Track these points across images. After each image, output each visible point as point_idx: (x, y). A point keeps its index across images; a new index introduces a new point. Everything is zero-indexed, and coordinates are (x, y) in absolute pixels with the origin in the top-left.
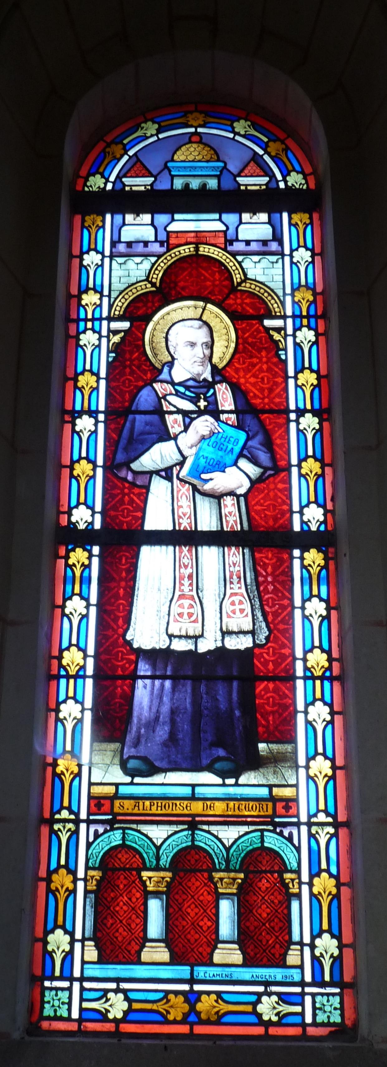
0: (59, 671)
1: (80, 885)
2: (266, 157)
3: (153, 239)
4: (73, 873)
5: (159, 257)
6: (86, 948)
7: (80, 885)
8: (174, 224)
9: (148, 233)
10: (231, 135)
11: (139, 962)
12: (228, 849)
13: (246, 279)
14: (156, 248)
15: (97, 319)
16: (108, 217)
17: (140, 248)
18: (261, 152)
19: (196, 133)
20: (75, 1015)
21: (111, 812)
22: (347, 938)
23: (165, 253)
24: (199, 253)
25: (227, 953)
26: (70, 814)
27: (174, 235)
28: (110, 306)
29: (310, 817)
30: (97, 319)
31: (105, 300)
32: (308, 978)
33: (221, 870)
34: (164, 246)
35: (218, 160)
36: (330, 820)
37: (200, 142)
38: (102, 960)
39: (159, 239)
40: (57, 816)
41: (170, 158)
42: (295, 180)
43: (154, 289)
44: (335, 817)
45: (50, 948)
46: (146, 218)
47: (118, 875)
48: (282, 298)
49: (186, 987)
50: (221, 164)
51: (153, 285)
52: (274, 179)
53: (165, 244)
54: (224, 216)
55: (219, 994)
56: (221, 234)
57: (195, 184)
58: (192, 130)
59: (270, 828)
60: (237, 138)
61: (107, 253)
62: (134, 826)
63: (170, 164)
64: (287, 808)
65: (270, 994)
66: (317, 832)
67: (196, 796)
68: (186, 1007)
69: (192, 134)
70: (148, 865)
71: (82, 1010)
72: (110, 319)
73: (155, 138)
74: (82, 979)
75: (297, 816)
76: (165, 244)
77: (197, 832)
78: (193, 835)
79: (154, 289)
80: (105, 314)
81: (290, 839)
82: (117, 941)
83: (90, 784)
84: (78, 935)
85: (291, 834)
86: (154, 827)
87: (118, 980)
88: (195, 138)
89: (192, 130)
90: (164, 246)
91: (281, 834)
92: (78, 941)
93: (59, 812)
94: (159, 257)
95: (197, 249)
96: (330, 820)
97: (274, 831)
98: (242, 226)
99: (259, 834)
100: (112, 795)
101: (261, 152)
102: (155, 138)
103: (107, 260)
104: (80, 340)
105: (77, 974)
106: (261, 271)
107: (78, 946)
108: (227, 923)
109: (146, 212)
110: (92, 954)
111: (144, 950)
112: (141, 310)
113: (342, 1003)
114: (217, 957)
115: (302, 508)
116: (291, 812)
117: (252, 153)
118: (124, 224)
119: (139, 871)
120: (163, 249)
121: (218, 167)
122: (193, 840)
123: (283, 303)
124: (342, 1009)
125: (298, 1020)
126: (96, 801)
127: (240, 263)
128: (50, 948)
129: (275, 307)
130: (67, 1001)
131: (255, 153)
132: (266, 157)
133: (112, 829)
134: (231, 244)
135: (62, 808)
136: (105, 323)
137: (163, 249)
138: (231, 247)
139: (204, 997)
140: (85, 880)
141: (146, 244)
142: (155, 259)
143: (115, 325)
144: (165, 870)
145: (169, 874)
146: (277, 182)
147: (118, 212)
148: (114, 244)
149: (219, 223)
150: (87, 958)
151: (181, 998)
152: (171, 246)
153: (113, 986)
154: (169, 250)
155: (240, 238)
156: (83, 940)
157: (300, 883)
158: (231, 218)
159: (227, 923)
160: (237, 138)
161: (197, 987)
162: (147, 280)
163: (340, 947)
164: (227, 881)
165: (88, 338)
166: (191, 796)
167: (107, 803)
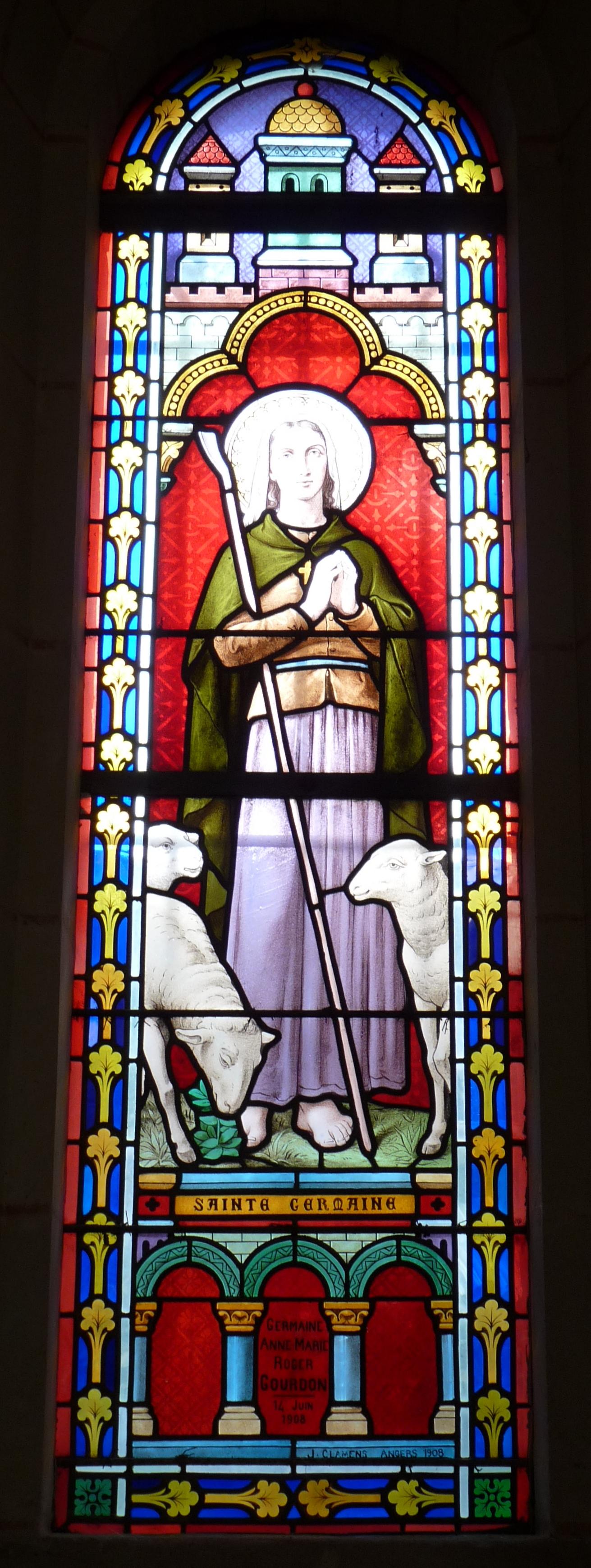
0: (87, 1003)
1: (125, 1323)
2: (423, 129)
3: (232, 280)
4: (116, 1306)
5: (242, 310)
6: (134, 1416)
7: (125, 1323)
8: (269, 252)
9: (223, 270)
10: (365, 84)
11: (214, 1435)
12: (347, 1266)
13: (386, 351)
14: (236, 295)
15: (141, 418)
16: (158, 237)
17: (208, 295)
18: (415, 118)
19: (305, 79)
20: (121, 1512)
21: (171, 1215)
22: (522, 1398)
23: (251, 305)
24: (309, 304)
25: (347, 1422)
26: (108, 1220)
27: (267, 272)
28: (163, 394)
29: (471, 1217)
30: (141, 418)
31: (154, 389)
32: (465, 1453)
33: (336, 1299)
34: (250, 293)
35: (343, 134)
36: (500, 1224)
37: (313, 96)
38: (158, 1435)
39: (241, 281)
40: (89, 1223)
41: (262, 129)
42: (470, 176)
43: (234, 367)
44: (508, 1218)
45: (81, 1417)
46: (220, 241)
47: (182, 1301)
48: (443, 387)
49: (286, 1470)
50: (347, 142)
51: (232, 359)
52: (434, 172)
53: (253, 289)
54: (350, 237)
55: (333, 1479)
56: (345, 273)
57: (304, 182)
58: (300, 72)
59: (413, 1235)
60: (377, 90)
61: (156, 305)
62: (208, 1236)
63: (262, 141)
64: (438, 1204)
65: (408, 1477)
66: (483, 1243)
67: (302, 1186)
68: (283, 1500)
69: (299, 80)
70: (227, 1294)
71: (130, 1505)
72: (162, 419)
73: (236, 88)
74: (130, 1461)
75: (453, 1216)
76: (253, 289)
77: (300, 1242)
78: (295, 1246)
79: (234, 367)
80: (154, 412)
81: (442, 1252)
82: (183, 1406)
83: (139, 1171)
84: (123, 1398)
85: (444, 1243)
86: (237, 1236)
87: (182, 1460)
88: (304, 89)
89: (300, 72)
90: (250, 293)
91: (429, 1244)
92: (123, 1405)
93: (91, 1216)
94: (242, 310)
95: (306, 299)
96: (500, 1224)
97: (417, 1240)
98: (380, 260)
99: (394, 1242)
100: (171, 1186)
101: (415, 118)
102: (236, 88)
103: (156, 318)
104: (82, 1319)
105: (122, 1453)
106: (412, 338)
107: (123, 1412)
108: (345, 1383)
109: (220, 230)
110: (143, 1425)
111: (223, 1417)
112: (210, 409)
113: (513, 1490)
114: (332, 1428)
115: (466, 665)
116: (446, 1210)
117: (399, 121)
118: (185, 253)
119: (213, 1301)
120: (250, 298)
121: (342, 148)
122: (295, 1253)
123: (444, 396)
124: (513, 1499)
125: (450, 1513)
126: (148, 1198)
127: (376, 327)
128: (84, 1326)
129: (433, 405)
130: (109, 1493)
131: (407, 120)
132: (423, 129)
133: (172, 1240)
134: (361, 291)
135: (95, 1210)
136: (153, 425)
137: (250, 298)
138: (360, 296)
139: (311, 1484)
140: (132, 1316)
141: (221, 288)
142: (235, 314)
143: (171, 428)
144: (252, 1300)
145: (260, 1306)
146: (441, 177)
147: (175, 230)
148: (166, 288)
149: (341, 252)
150: (136, 1432)
151: (276, 1486)
152: (261, 293)
153: (176, 1469)
154: (258, 300)
155: (376, 281)
156: (130, 1405)
157: (457, 1316)
158: (362, 243)
159: (345, 1383)
160: (377, 90)
161: (301, 1470)
162: (223, 350)
163: (513, 1408)
164: (346, 1315)
165: (125, 456)
166: (291, 1186)
167: (164, 1200)
